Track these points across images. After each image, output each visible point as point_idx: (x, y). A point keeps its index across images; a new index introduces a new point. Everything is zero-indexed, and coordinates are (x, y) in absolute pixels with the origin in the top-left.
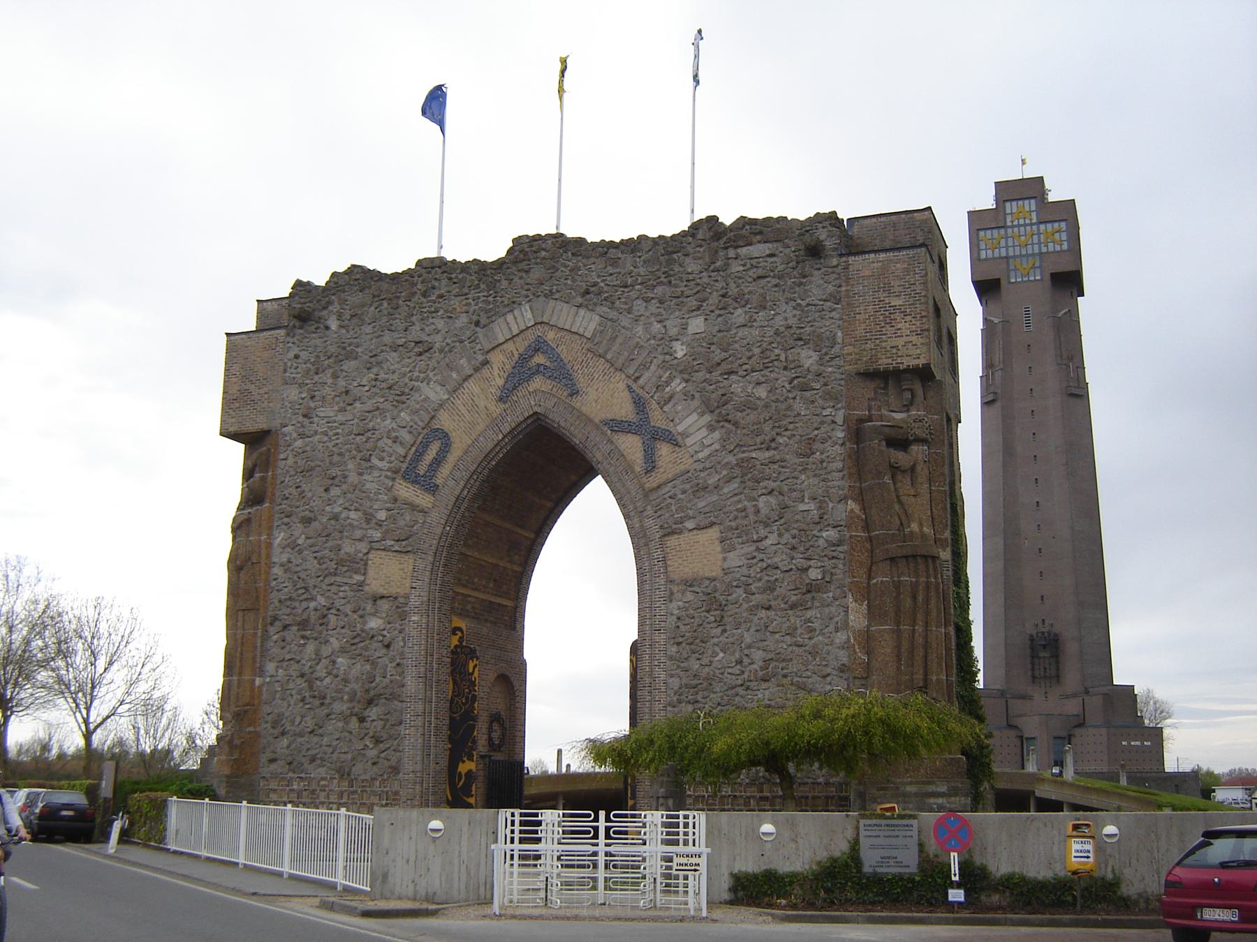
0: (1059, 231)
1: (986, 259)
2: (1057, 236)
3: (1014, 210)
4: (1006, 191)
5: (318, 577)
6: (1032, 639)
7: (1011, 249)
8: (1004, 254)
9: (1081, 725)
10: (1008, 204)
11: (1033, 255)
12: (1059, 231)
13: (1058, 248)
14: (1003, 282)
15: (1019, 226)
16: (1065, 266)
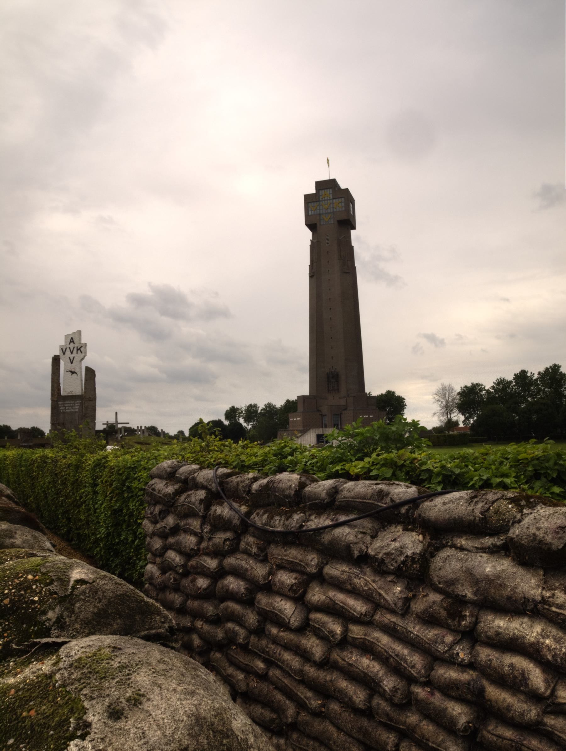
0: (341, 202)
1: (311, 215)
2: (340, 205)
3: (323, 193)
4: (320, 185)
6: (328, 374)
7: (321, 211)
8: (318, 213)
9: (346, 409)
10: (321, 192)
11: (330, 213)
12: (341, 202)
13: (341, 209)
14: (318, 225)
15: (325, 200)
16: (343, 217)
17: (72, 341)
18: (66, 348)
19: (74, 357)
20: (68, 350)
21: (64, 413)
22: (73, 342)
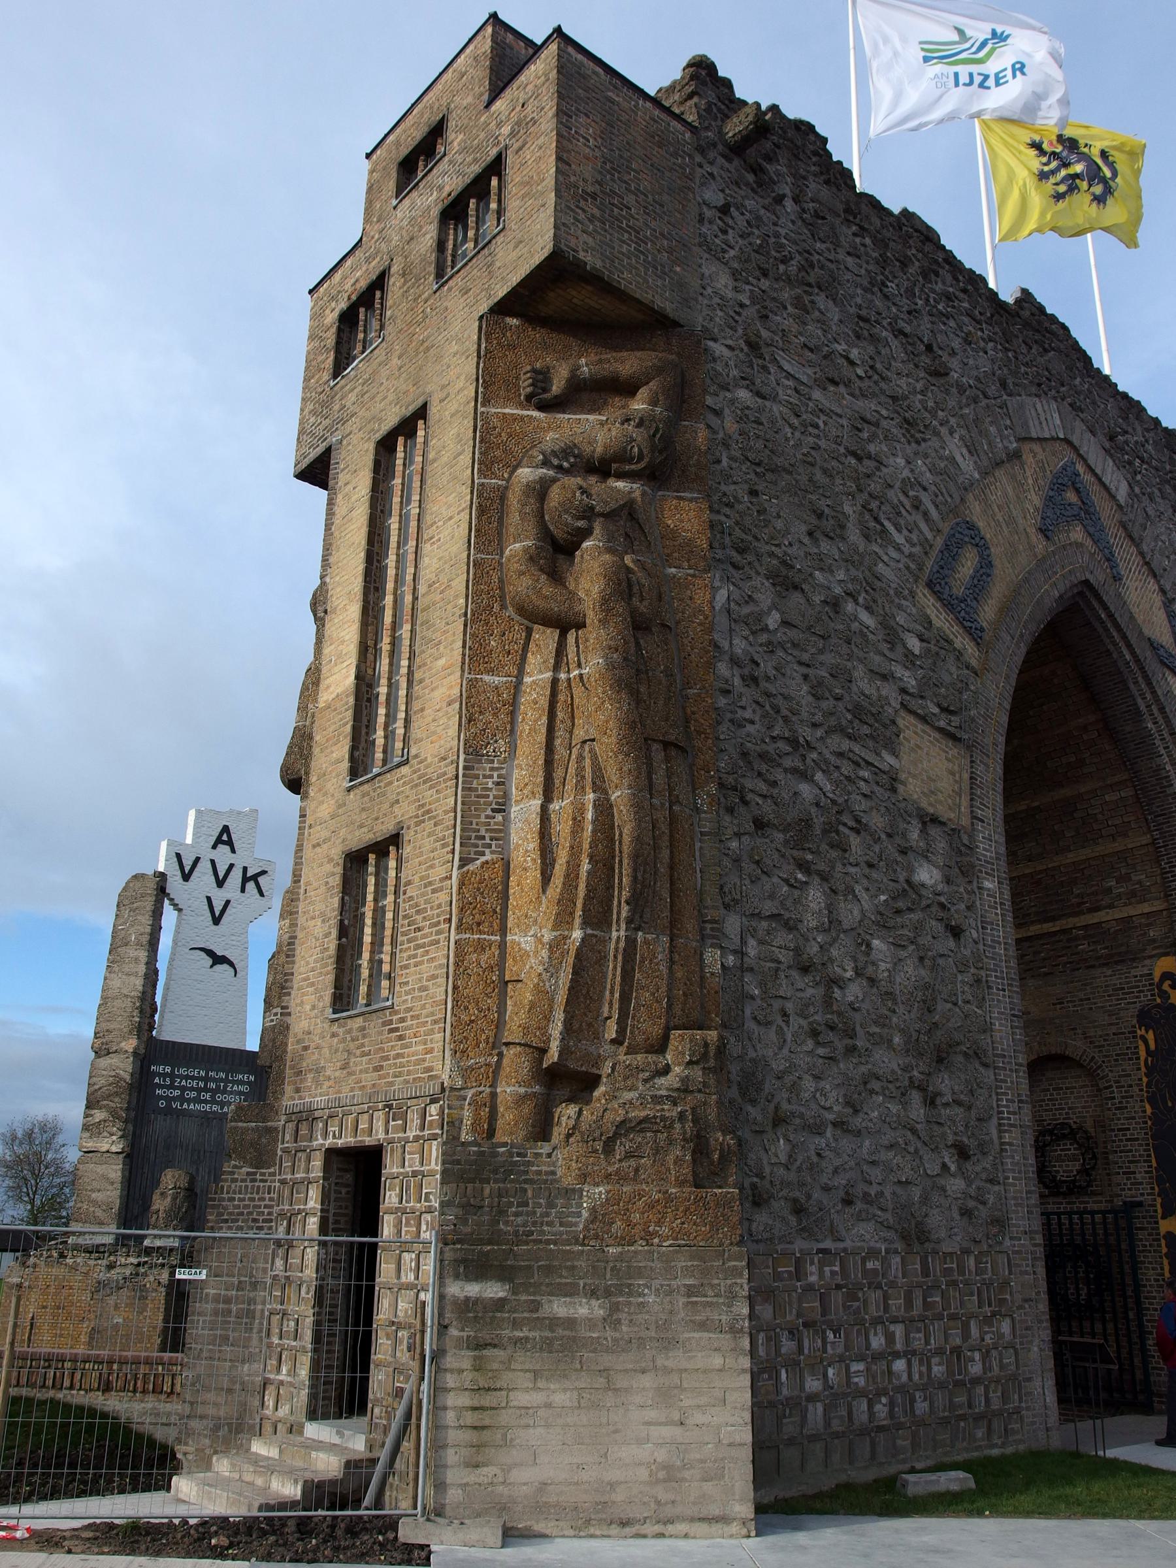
5: (815, 725)
17: (224, 838)
18: (198, 859)
19: (228, 902)
20: (204, 867)
21: (168, 1111)
22: (230, 843)
